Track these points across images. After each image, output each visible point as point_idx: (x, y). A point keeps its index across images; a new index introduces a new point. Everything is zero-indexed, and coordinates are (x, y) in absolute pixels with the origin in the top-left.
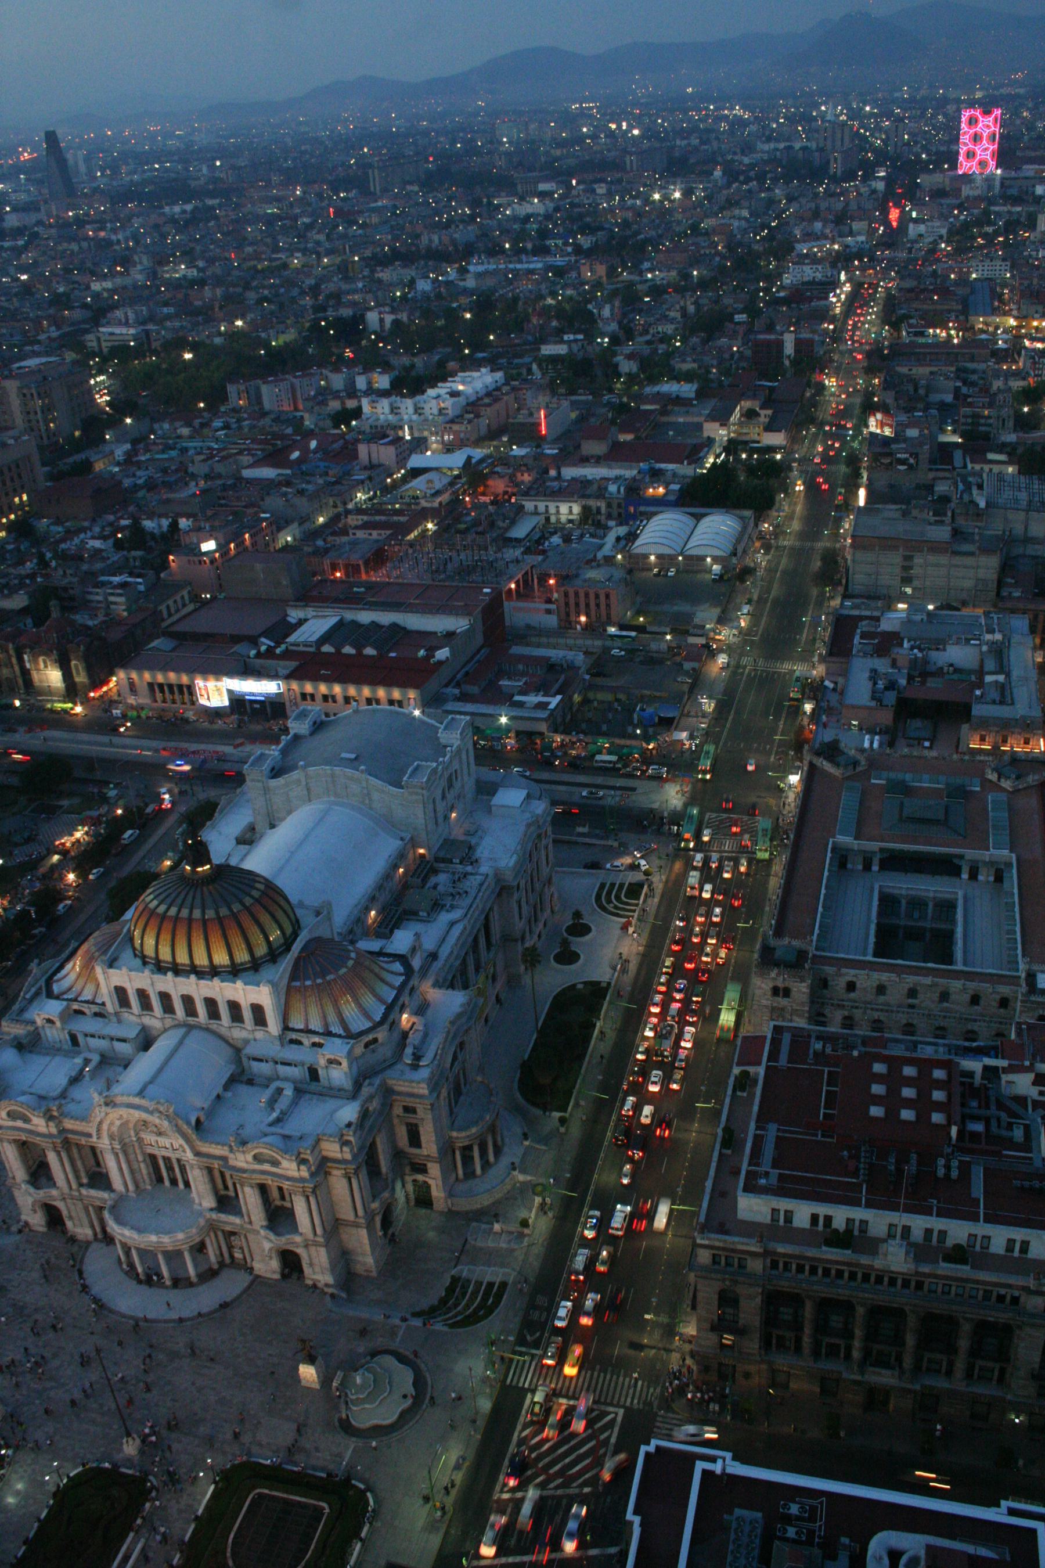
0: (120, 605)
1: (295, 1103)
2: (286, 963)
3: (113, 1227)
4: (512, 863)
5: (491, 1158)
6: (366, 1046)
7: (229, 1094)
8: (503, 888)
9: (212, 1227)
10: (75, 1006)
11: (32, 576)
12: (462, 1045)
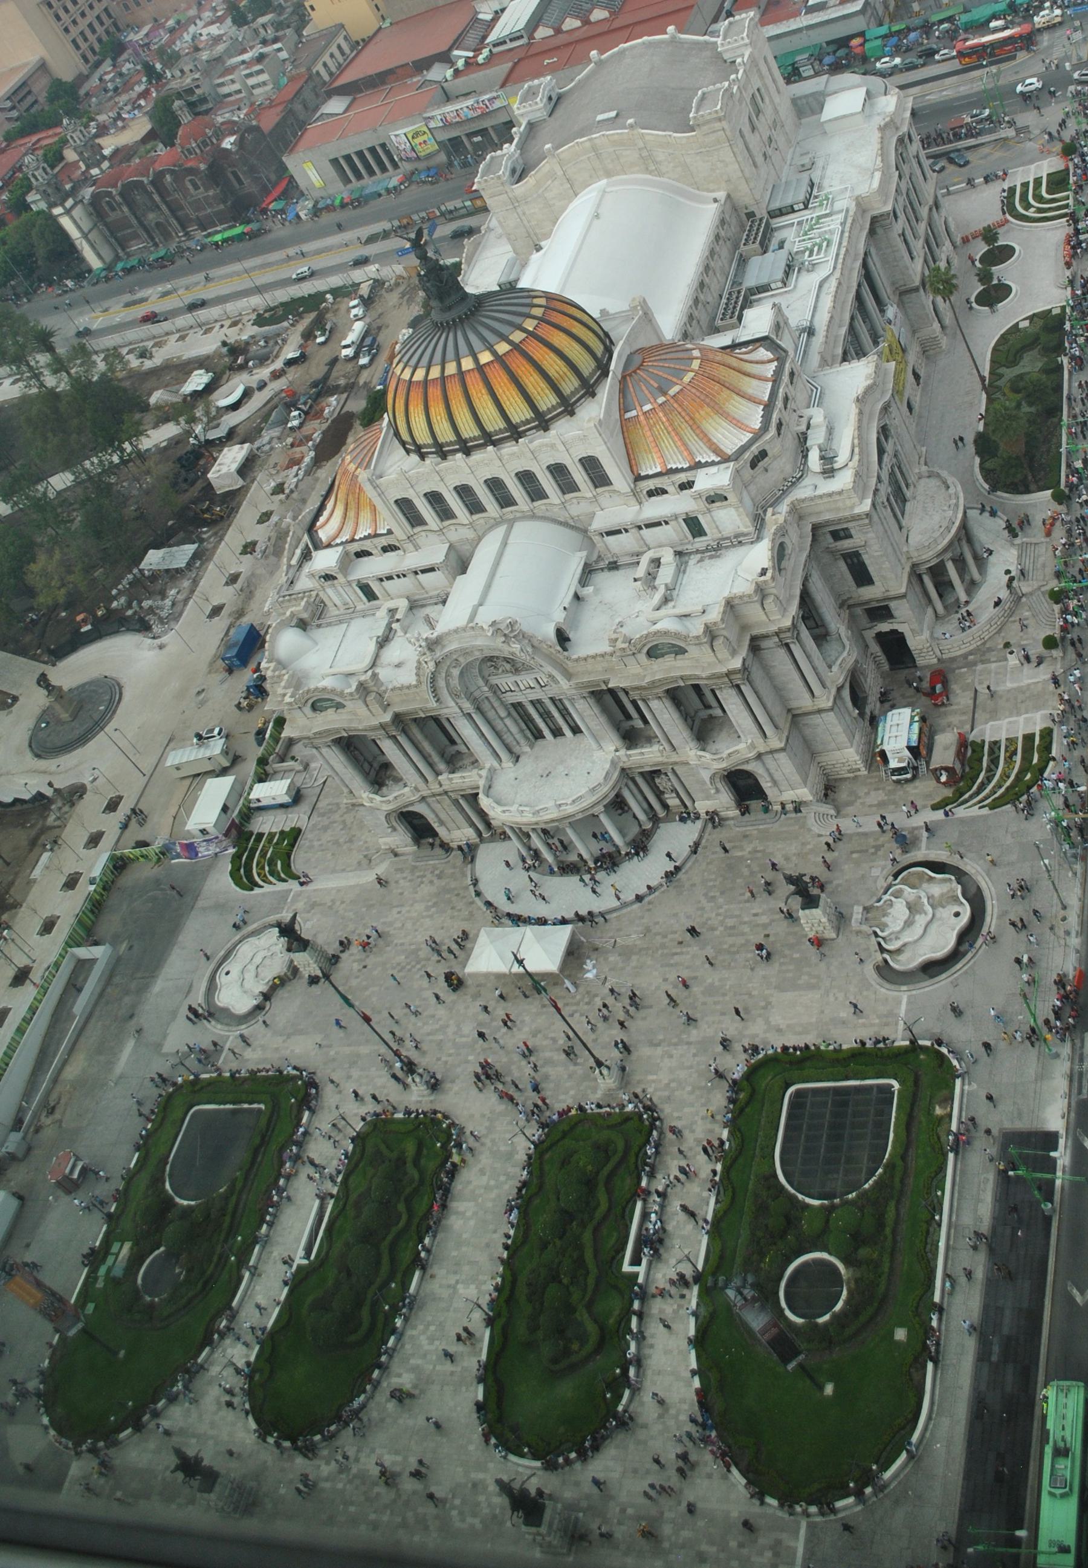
2: (607, 390)
4: (876, 184)
6: (754, 464)
7: (589, 590)
10: (355, 547)
11: (145, 94)
12: (884, 431)
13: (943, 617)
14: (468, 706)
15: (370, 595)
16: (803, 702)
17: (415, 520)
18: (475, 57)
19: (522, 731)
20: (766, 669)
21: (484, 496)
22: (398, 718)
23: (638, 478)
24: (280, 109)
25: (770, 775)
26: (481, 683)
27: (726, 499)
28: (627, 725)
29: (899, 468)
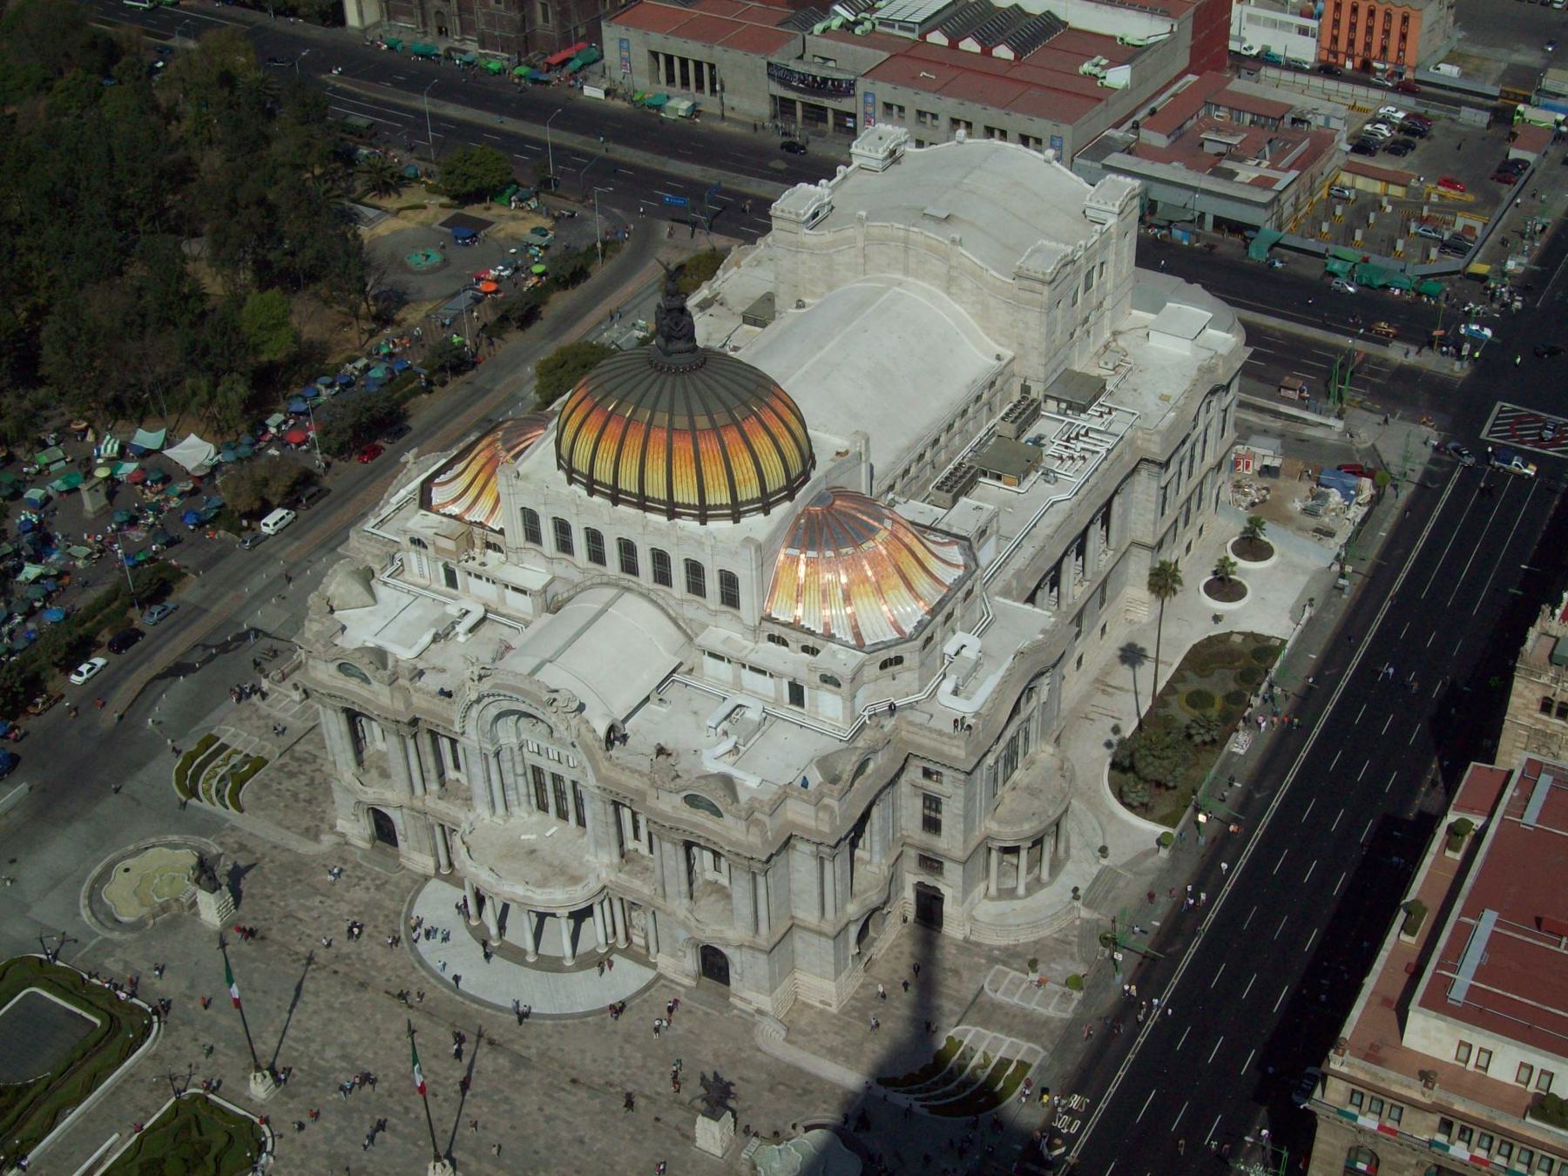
5: (1045, 875)
6: (884, 666)
13: (992, 899)
17: (533, 535)
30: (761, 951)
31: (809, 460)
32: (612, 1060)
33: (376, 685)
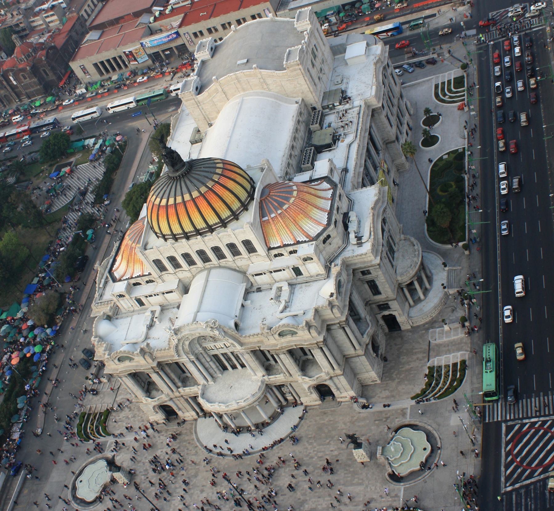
0: (54, 20)
1: (292, 293)
2: (254, 207)
3: (207, 406)
4: (373, 93)
6: (324, 242)
7: (248, 302)
8: (373, 110)
9: (268, 387)
10: (133, 281)
12: (384, 221)
13: (414, 306)
14: (192, 358)
15: (141, 303)
16: (350, 351)
18: (164, 10)
19: (217, 367)
20: (333, 338)
21: (196, 258)
22: (160, 364)
23: (270, 249)
24: (65, 34)
25: (336, 386)
26: (198, 346)
27: (312, 259)
28: (268, 363)
29: (391, 236)
30: (340, 375)
31: (251, 181)
32: (307, 448)
33: (136, 358)
